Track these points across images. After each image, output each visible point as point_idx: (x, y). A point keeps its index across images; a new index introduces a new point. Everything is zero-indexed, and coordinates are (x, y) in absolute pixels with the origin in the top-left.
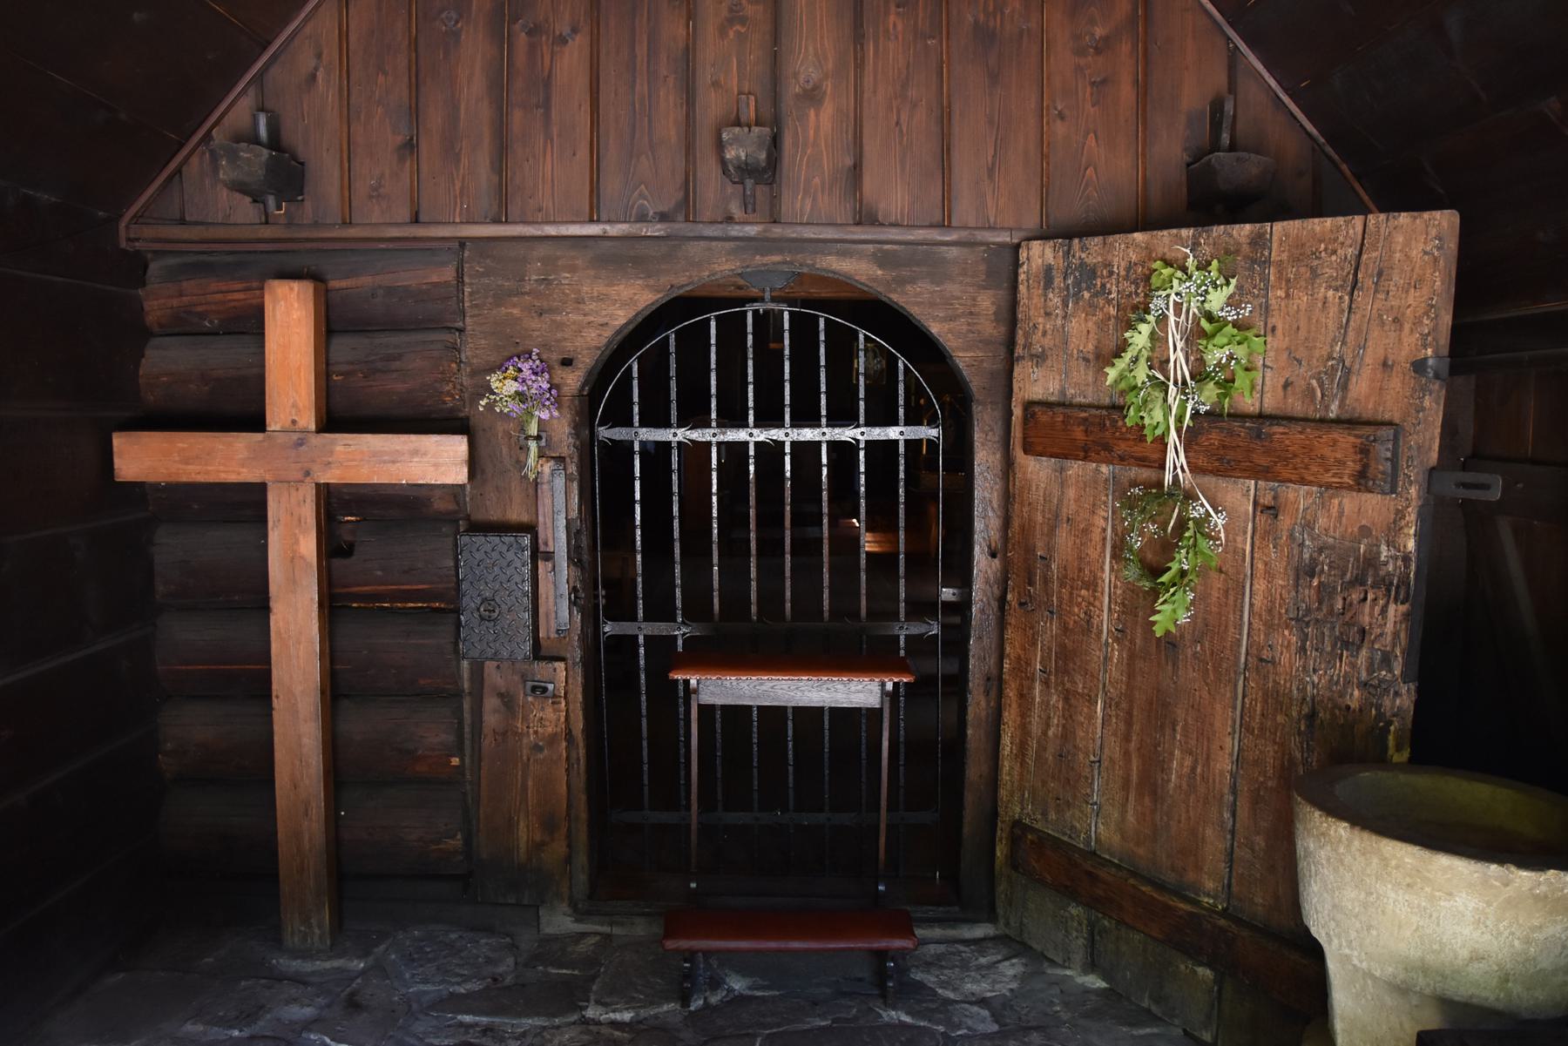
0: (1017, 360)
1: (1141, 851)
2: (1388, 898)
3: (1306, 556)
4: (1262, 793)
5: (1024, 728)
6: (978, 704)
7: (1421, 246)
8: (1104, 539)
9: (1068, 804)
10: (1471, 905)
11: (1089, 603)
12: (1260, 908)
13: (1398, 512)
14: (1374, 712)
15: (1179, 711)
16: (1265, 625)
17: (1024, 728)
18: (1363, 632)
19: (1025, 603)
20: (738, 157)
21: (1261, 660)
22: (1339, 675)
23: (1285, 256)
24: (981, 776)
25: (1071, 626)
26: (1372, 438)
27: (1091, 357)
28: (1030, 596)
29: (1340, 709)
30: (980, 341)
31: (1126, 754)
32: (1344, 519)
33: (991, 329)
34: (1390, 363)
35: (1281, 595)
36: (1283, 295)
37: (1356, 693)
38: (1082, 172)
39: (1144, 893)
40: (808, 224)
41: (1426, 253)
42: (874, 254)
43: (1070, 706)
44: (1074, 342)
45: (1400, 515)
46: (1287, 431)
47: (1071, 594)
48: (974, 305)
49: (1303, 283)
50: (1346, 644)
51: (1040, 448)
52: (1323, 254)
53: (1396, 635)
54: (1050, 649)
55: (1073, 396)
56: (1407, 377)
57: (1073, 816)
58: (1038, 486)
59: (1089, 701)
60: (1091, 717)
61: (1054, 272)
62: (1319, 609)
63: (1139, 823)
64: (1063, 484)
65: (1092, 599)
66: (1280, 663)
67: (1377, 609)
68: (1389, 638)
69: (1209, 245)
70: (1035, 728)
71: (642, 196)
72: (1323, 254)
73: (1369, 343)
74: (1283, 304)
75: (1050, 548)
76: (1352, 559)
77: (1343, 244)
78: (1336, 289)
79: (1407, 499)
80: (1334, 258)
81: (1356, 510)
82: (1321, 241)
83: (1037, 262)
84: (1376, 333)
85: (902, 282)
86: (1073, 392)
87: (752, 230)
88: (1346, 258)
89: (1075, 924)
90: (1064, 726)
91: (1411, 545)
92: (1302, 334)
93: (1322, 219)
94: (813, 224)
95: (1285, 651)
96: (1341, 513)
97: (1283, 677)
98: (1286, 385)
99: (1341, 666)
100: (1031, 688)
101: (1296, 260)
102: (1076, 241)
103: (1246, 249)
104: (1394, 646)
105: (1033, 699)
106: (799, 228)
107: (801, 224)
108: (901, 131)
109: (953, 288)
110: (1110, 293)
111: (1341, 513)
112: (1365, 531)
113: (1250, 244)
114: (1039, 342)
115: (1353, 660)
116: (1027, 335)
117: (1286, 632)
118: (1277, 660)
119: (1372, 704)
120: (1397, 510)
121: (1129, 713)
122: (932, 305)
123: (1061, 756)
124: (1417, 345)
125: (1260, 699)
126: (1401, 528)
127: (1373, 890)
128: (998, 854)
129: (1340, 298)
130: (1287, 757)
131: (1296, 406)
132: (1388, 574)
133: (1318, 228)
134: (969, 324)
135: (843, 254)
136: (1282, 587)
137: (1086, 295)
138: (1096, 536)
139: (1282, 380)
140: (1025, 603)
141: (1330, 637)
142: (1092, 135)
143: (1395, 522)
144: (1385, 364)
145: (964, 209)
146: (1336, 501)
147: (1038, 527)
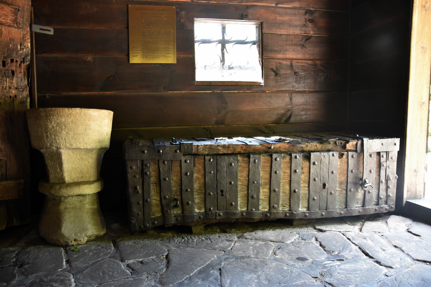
10: (107, 121)
13: (24, 35)
22: (6, 87)
37: (14, 92)
53: (24, 72)
67: (18, 64)
68: (23, 73)
76: (6, 49)
79: (27, 31)
81: (8, 32)
99: (6, 84)
115: (11, 81)
120: (24, 34)
126: (26, 40)
127: (88, 124)
143: (23, 37)
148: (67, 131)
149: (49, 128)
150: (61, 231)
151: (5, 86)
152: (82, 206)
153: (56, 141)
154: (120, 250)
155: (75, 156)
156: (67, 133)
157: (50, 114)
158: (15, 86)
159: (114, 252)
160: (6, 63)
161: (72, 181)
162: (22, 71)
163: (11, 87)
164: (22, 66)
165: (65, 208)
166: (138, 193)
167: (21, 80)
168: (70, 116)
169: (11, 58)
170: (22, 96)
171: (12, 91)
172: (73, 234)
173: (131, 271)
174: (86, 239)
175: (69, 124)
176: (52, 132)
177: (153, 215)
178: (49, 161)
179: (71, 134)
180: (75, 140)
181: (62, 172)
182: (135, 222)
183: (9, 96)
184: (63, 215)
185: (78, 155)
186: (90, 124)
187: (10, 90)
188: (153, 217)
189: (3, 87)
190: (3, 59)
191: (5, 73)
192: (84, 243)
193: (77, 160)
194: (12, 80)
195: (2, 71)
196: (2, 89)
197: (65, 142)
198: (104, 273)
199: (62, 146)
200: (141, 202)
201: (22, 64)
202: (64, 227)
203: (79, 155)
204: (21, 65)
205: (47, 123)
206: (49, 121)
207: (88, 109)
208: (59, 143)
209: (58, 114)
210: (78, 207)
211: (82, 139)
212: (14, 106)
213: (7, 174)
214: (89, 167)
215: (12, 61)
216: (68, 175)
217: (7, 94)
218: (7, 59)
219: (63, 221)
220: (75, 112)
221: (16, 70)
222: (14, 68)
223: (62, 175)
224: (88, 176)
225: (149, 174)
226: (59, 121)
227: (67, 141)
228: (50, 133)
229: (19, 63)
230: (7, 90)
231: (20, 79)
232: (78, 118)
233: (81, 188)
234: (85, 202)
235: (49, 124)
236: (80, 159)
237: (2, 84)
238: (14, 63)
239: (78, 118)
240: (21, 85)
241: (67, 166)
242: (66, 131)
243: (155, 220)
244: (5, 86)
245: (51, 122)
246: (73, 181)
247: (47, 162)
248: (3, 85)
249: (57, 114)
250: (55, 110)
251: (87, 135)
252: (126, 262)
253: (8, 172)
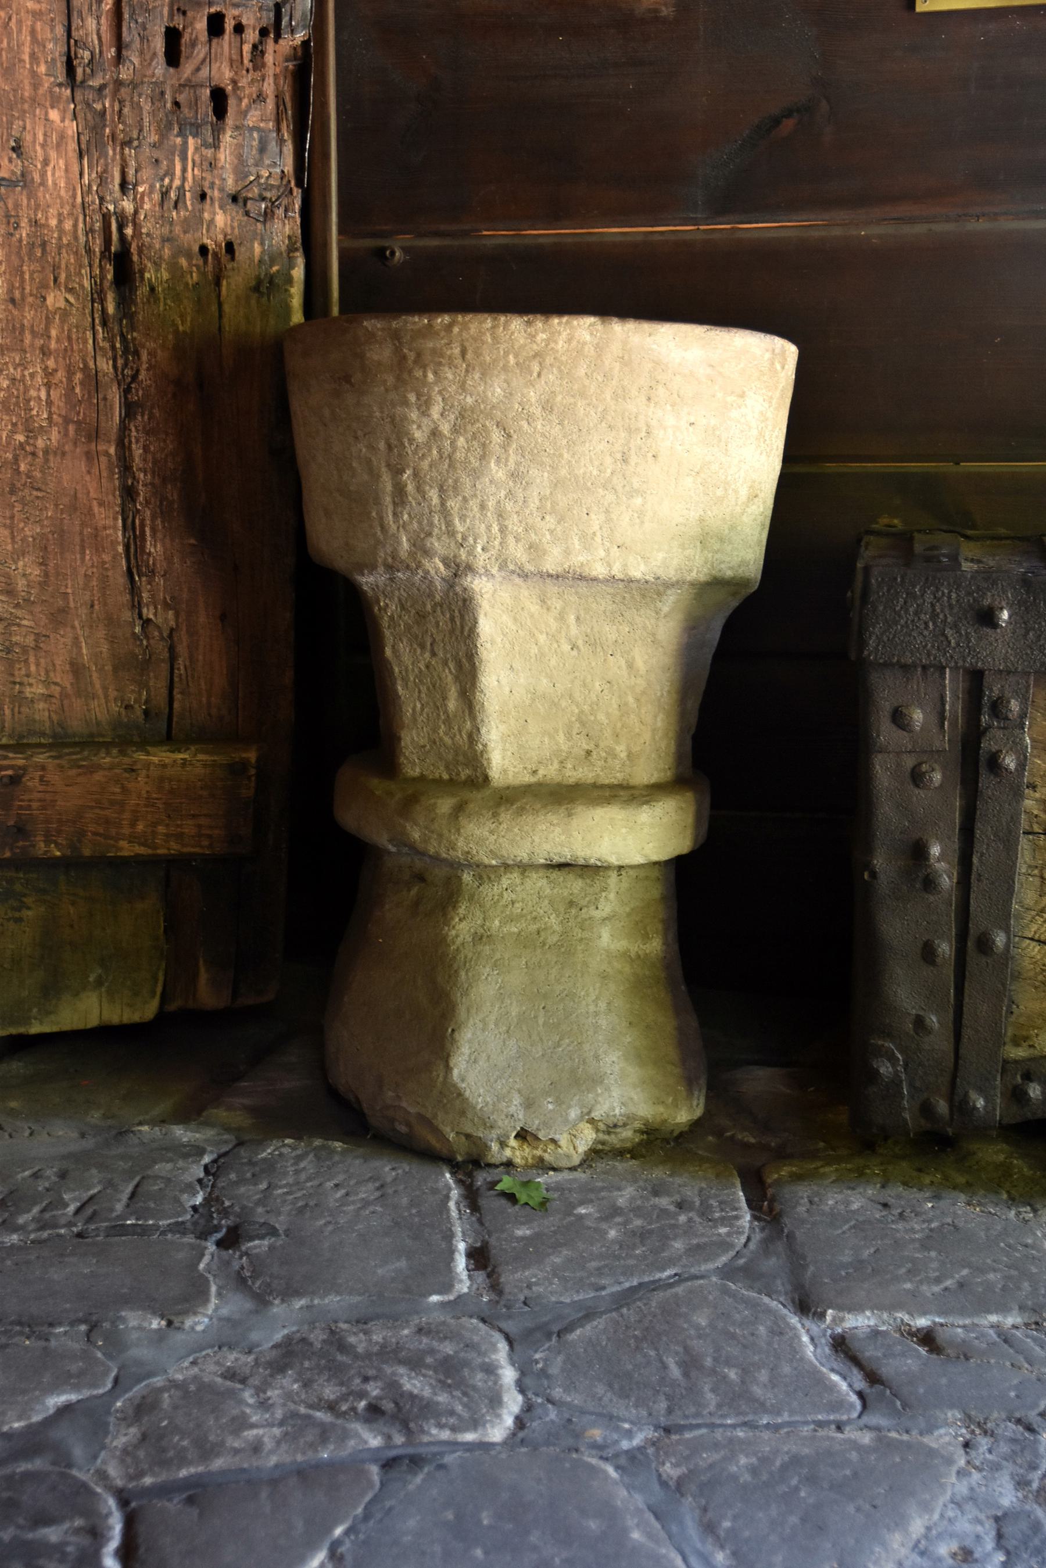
2: (665, 429)
4: (23, 467)
12: (41, 705)
22: (181, 189)
29: (189, 256)
35: (33, 32)
37: (220, 219)
62: (119, 58)
66: (43, 183)
67: (247, 48)
68: (270, 104)
95: (53, 154)
99: (184, 170)
115: (209, 153)
117: (54, 115)
118: (37, 178)
127: (642, 425)
130: (79, 376)
136: (37, 15)
141: (153, 113)
148: (518, 464)
149: (411, 440)
150: (448, 1069)
151: (177, 183)
152: (578, 933)
153: (449, 524)
154: (790, 1237)
155: (554, 625)
156: (514, 475)
157: (419, 355)
158: (231, 184)
159: (752, 1246)
160: (186, 39)
161: (528, 779)
162: (269, 88)
163: (209, 192)
164: (269, 58)
165: (478, 938)
166: (929, 883)
167: (262, 149)
168: (536, 368)
169: (213, 10)
170: (262, 244)
171: (214, 214)
172: (517, 1100)
173: (860, 1384)
174: (587, 1137)
175: (530, 419)
176: (425, 464)
177: (1016, 1042)
178: (403, 647)
179: (540, 478)
180: (561, 520)
181: (473, 717)
182: (896, 1072)
183: (196, 248)
184: (463, 974)
185: (572, 618)
186: (654, 423)
187: (202, 211)
188: (1019, 1053)
189: (165, 194)
190: (171, 16)
191: (177, 104)
192: (576, 1160)
193: (566, 647)
194: (216, 146)
195: (163, 93)
196: (162, 204)
197: (503, 530)
198: (690, 1363)
199: (481, 559)
200: (945, 948)
201: (270, 45)
202: (465, 1050)
203: (578, 619)
204: (263, 53)
205: (399, 410)
206: (412, 398)
207: (646, 326)
208: (464, 538)
209: (469, 355)
210: (553, 939)
211: (602, 517)
212: (220, 305)
213: (176, 705)
214: (630, 699)
215: (216, 26)
216: (504, 738)
217: (189, 236)
218: (189, 14)
219: (462, 1012)
220: (569, 340)
221: (234, 82)
222: (223, 74)
223: (473, 736)
224: (623, 755)
225: (1012, 766)
226: (469, 400)
227: (514, 524)
228: (416, 474)
229: (251, 36)
230: (187, 210)
231: (255, 143)
232: (587, 382)
233: (575, 822)
234: (597, 914)
235: (414, 415)
236: (580, 643)
237: (162, 172)
238: (226, 37)
239: (587, 382)
240: (258, 177)
241: (504, 682)
242: (511, 465)
243: (1028, 1077)
244: (177, 183)
245: (424, 407)
246: (533, 780)
247: (388, 652)
248: (167, 181)
249: (463, 353)
250: (449, 328)
251: (633, 493)
252: (829, 1318)
253: (177, 696)
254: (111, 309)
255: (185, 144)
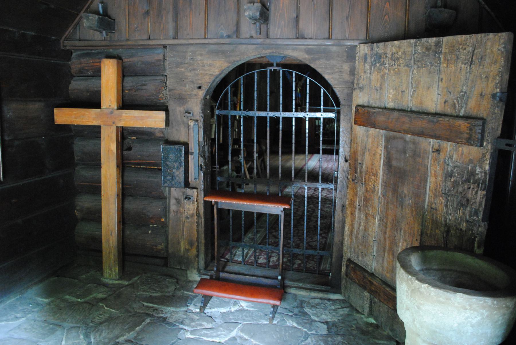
0: (354, 89)
1: (388, 275)
3: (450, 169)
5: (352, 225)
6: (339, 215)
7: (497, 47)
8: (380, 158)
9: (365, 255)
11: (375, 181)
13: (483, 154)
14: (470, 232)
15: (402, 225)
16: (434, 195)
17: (352, 225)
18: (468, 200)
19: (354, 180)
20: (249, 15)
21: (432, 208)
22: (459, 216)
23: (447, 51)
24: (339, 241)
25: (368, 190)
26: (474, 124)
27: (378, 89)
28: (356, 177)
30: (344, 82)
31: (385, 238)
32: (463, 156)
33: (346, 77)
34: (483, 94)
36: (446, 66)
37: (465, 224)
38: (383, 17)
39: (387, 291)
40: (279, 38)
41: (499, 50)
42: (305, 50)
43: (367, 219)
44: (373, 83)
45: (484, 155)
46: (443, 120)
47: (369, 177)
48: (342, 69)
49: (453, 61)
50: (462, 205)
51: (359, 123)
52: (461, 50)
53: (480, 203)
54: (361, 198)
55: (372, 104)
56: (489, 100)
57: (367, 259)
58: (359, 137)
59: (373, 218)
60: (374, 224)
61: (368, 56)
62: (453, 190)
63: (388, 265)
64: (368, 136)
65: (375, 180)
67: (474, 192)
68: (478, 204)
69: (420, 46)
70: (356, 226)
71: (222, 29)
72: (461, 50)
73: (476, 86)
74: (446, 70)
75: (362, 160)
77: (468, 46)
78: (465, 64)
80: (465, 51)
81: (468, 152)
82: (460, 45)
83: (362, 52)
84: (479, 82)
85: (315, 59)
86: (372, 102)
87: (259, 41)
88: (469, 51)
89: (366, 299)
90: (365, 226)
91: (487, 168)
92: (452, 82)
93: (461, 36)
94: (281, 39)
96: (462, 154)
97: (439, 215)
98: (445, 102)
100: (355, 211)
101: (451, 52)
102: (375, 44)
103: (433, 47)
104: (479, 207)
105: (356, 215)
106: (276, 40)
107: (277, 39)
108: (314, 4)
109: (333, 62)
110: (386, 64)
111: (462, 154)
112: (471, 161)
113: (435, 45)
114: (362, 83)
115: (464, 211)
116: (358, 80)
119: (470, 230)
121: (386, 224)
122: (326, 68)
123: (364, 237)
124: (493, 87)
125: (431, 223)
126: (484, 161)
128: (343, 270)
129: (467, 67)
131: (449, 110)
132: (479, 179)
133: (459, 39)
134: (339, 76)
135: (293, 49)
136: (441, 181)
137: (378, 65)
138: (378, 156)
139: (444, 100)
140: (354, 180)
142: (388, 3)
143: (482, 158)
144: (481, 95)
145: (336, 33)
146: (461, 149)
147: (359, 152)
254: (445, 236)
255: (460, 209)
